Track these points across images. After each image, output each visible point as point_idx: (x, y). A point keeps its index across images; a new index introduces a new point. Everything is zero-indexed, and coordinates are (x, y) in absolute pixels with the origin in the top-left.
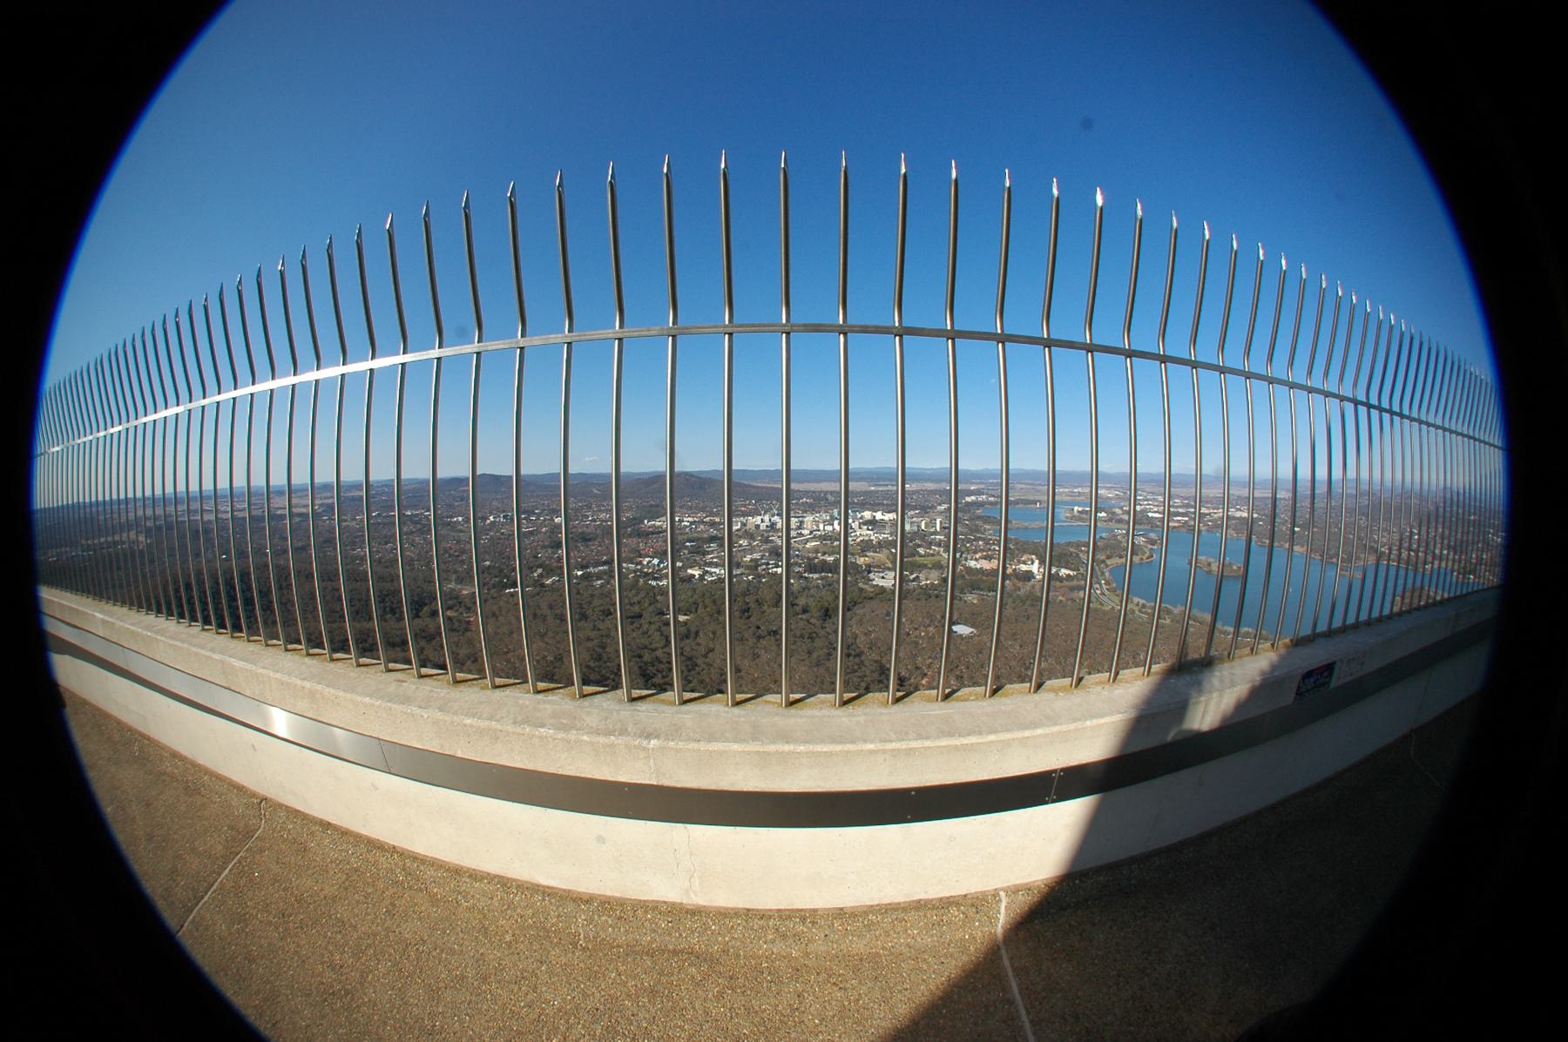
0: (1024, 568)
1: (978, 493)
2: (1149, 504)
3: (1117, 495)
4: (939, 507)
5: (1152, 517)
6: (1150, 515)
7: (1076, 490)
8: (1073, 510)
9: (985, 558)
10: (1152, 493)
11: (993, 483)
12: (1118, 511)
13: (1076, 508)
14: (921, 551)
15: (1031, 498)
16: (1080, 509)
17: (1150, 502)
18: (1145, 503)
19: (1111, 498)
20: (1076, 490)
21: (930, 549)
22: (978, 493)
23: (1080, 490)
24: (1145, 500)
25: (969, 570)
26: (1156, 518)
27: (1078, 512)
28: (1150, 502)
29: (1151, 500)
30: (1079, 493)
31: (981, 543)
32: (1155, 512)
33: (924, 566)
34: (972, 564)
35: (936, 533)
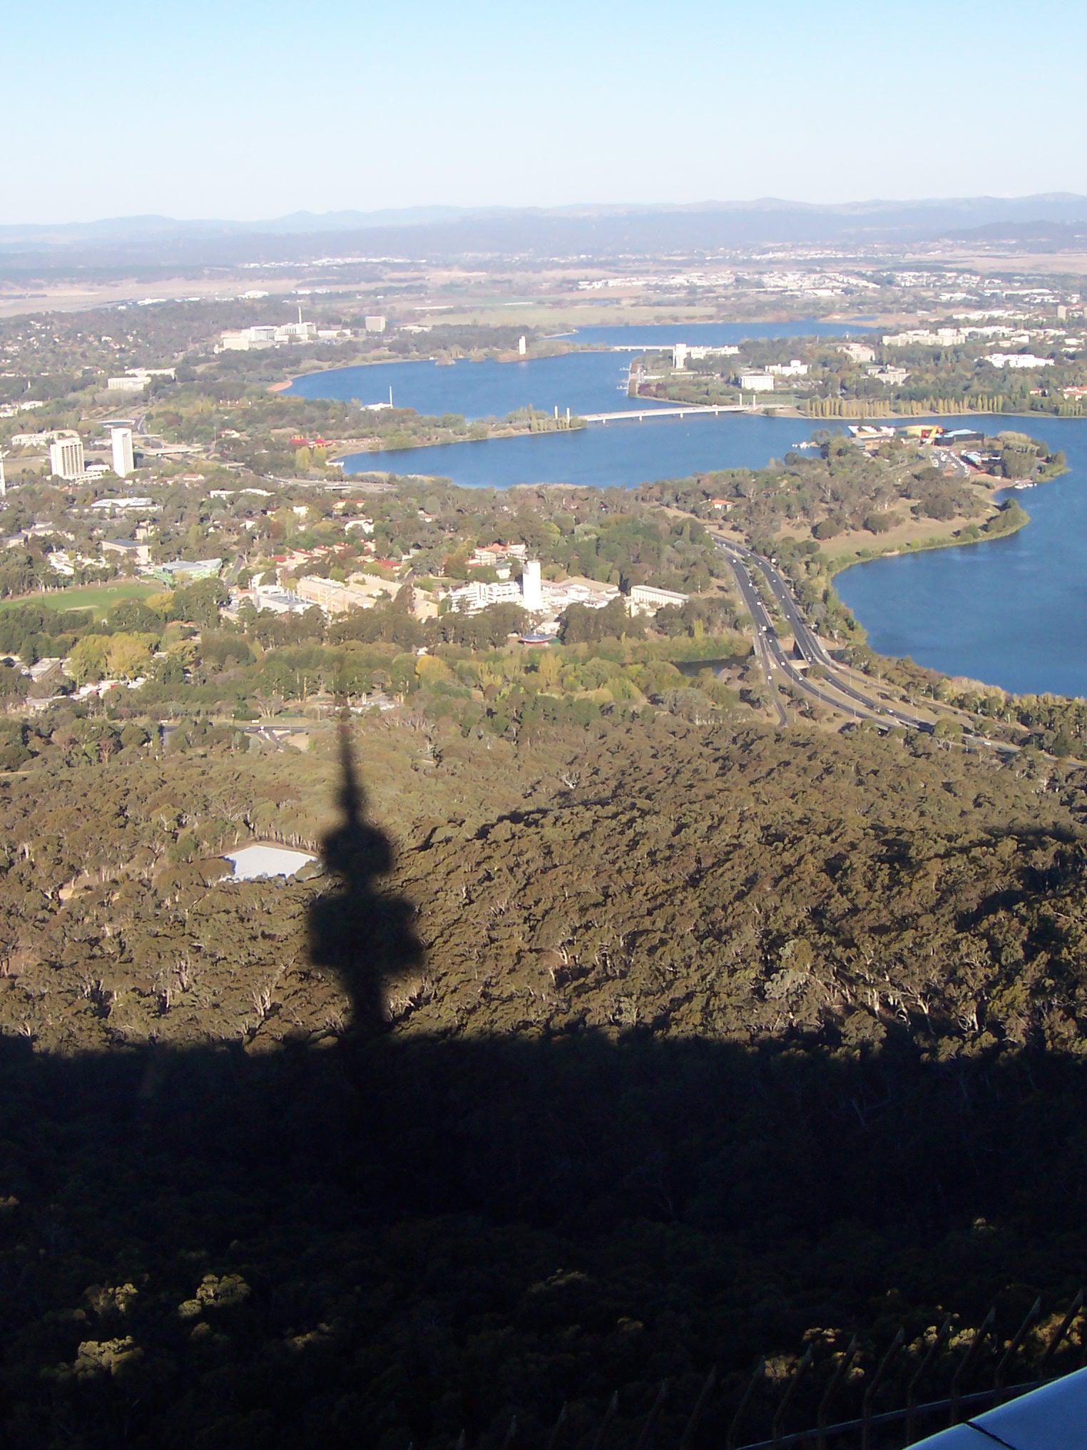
0: (479, 596)
1: (274, 311)
2: (992, 322)
3: (846, 291)
4: (114, 383)
5: (1007, 370)
6: (998, 361)
7: (679, 280)
8: (669, 357)
9: (322, 570)
10: (1008, 278)
11: (326, 269)
12: (861, 353)
13: (680, 352)
14: (61, 563)
15: (493, 320)
16: (699, 353)
17: (996, 313)
18: (976, 315)
19: (828, 308)
20: (679, 280)
21: (96, 552)
22: (274, 311)
23: (694, 277)
24: (967, 305)
25: (264, 624)
26: (1024, 371)
27: (690, 363)
28: (996, 313)
29: (1000, 304)
30: (692, 289)
31: (301, 511)
32: (1023, 351)
33: (81, 622)
34: (267, 597)
35: (110, 487)
